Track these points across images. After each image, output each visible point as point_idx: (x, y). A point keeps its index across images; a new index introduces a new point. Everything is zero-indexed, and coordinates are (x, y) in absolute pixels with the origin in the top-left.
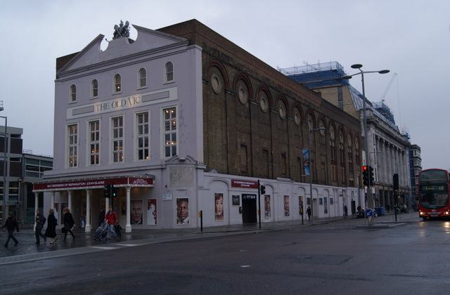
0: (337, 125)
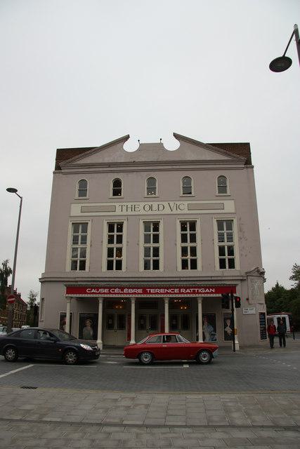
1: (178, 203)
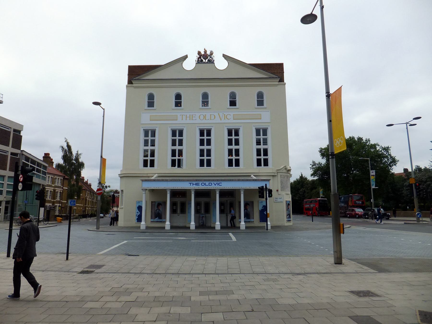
1: (226, 114)
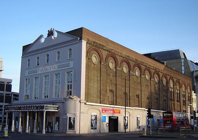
0: (175, 80)
1: (55, 65)
